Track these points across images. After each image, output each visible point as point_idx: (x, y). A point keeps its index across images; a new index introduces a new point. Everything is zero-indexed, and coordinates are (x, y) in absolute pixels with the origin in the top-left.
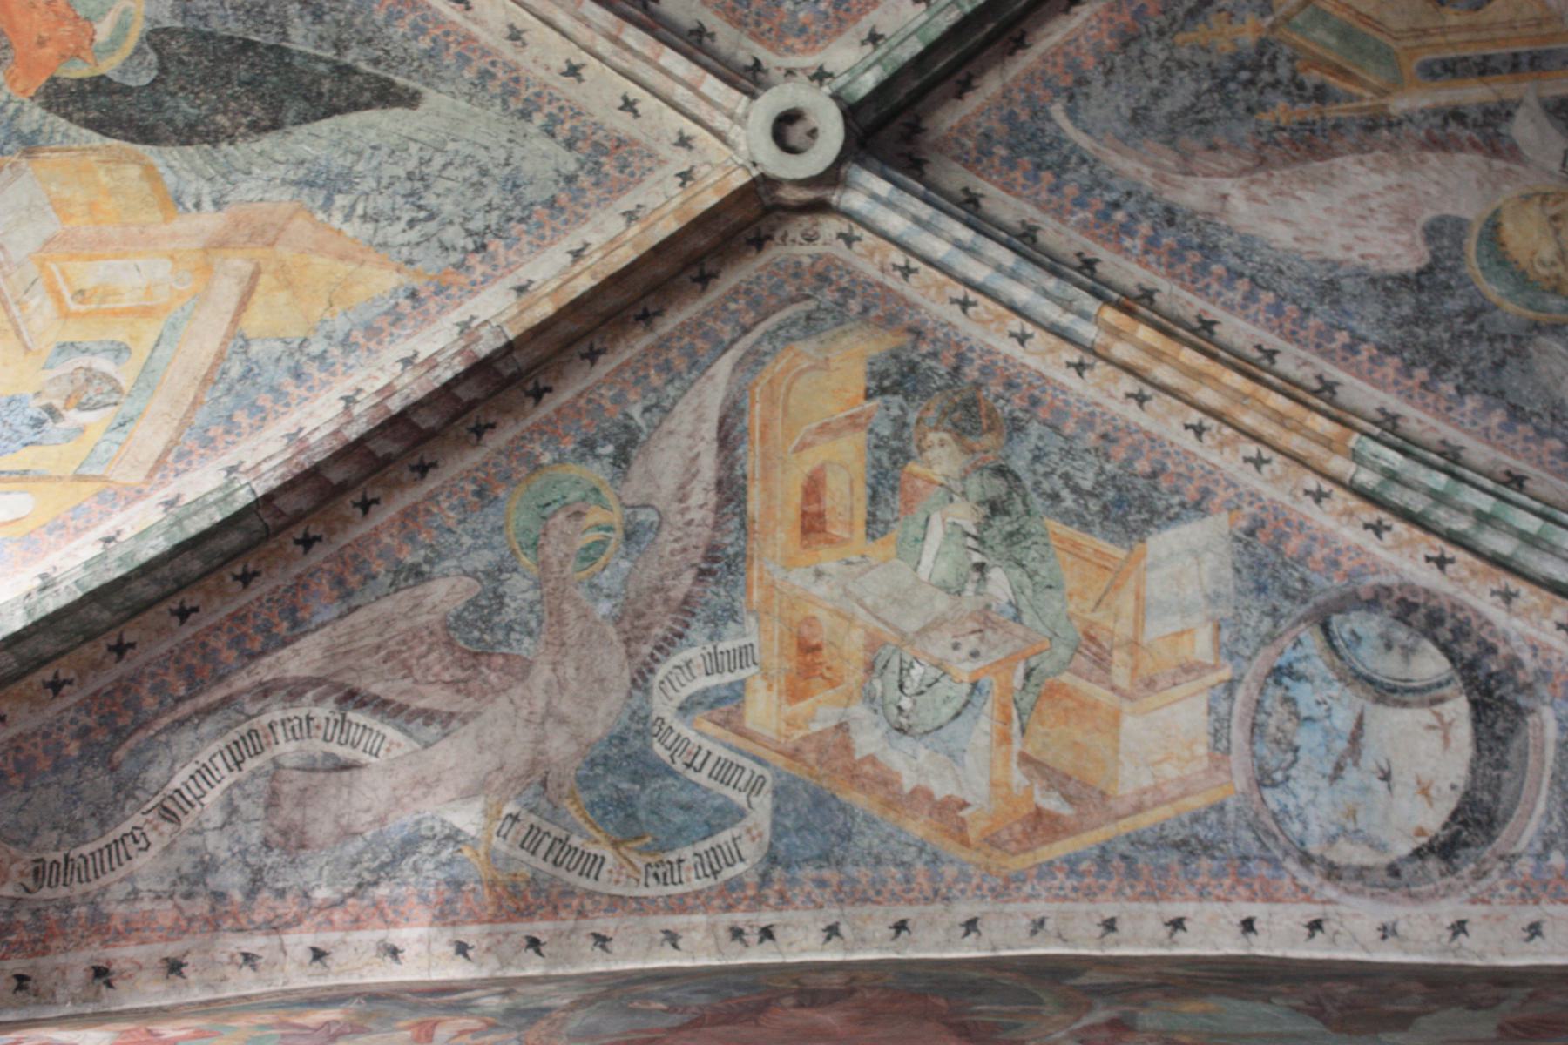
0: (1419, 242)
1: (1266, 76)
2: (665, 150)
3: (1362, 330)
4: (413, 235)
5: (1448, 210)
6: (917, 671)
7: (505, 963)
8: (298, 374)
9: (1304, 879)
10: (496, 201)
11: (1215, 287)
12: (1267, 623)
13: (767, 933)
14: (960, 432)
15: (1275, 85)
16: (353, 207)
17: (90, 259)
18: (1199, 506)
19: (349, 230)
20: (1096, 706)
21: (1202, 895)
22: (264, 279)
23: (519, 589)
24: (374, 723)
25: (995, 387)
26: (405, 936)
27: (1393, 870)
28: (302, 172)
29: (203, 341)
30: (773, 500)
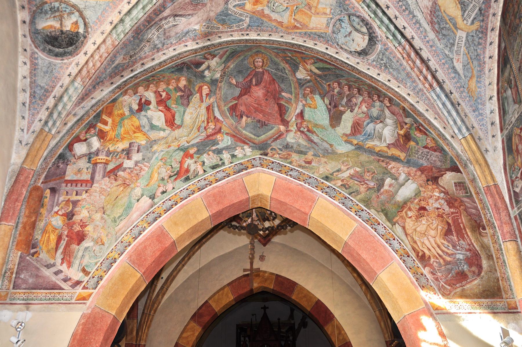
6: (277, 4)
7: (204, 43)
9: (337, 47)
20: (308, 14)
21: (320, 42)
24: (180, 18)
27: (351, 52)
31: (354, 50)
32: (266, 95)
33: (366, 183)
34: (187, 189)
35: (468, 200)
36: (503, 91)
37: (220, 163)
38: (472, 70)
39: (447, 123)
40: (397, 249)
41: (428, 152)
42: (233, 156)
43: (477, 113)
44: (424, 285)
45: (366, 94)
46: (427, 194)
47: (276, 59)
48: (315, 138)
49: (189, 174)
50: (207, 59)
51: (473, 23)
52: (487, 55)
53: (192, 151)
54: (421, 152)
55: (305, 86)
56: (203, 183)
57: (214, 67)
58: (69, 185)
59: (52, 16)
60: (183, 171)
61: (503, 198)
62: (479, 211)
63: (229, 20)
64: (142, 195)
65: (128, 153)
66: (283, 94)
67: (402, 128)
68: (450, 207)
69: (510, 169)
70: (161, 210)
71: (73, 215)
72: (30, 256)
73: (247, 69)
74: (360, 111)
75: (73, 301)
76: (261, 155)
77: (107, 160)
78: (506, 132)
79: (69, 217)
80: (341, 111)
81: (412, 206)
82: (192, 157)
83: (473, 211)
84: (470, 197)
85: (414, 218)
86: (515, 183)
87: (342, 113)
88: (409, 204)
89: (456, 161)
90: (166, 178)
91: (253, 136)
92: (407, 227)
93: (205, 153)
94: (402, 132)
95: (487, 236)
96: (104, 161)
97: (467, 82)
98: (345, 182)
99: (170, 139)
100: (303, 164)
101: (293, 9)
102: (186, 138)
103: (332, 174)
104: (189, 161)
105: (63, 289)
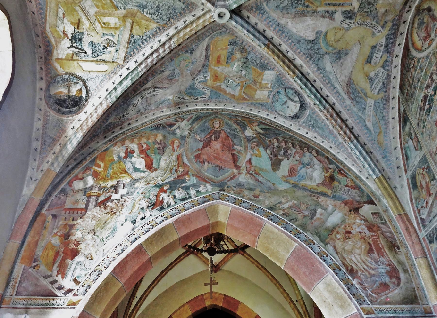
0: (315, 35)
1: (299, 2)
2: (199, 5)
3: (302, 50)
4: (158, 18)
5: (321, 29)
6: (231, 81)
8: (142, 43)
9: (275, 113)
10: (171, 12)
11: (283, 38)
12: (278, 86)
13: (208, 105)
14: (241, 52)
15: (300, 4)
16: (147, 12)
17: (104, 16)
18: (273, 69)
19: (147, 16)
22: (134, 24)
23: (177, 71)
24: (159, 90)
25: (247, 46)
26: (164, 110)
27: (286, 117)
28: (138, 4)
29: (126, 35)
30: (213, 58)
31: (288, 115)
32: (223, 147)
33: (302, 213)
34: (162, 216)
35: (384, 226)
36: (405, 142)
37: (188, 197)
38: (380, 128)
39: (362, 167)
40: (330, 264)
41: (349, 190)
42: (198, 192)
43: (385, 159)
44: (355, 293)
45: (298, 147)
46: (351, 221)
47: (230, 122)
48: (260, 179)
49: (164, 205)
50: (178, 121)
51: (378, 93)
52: (391, 117)
53: (166, 188)
54: (343, 189)
55: (252, 141)
56: (174, 211)
57: (183, 128)
58: (67, 212)
59: (63, 85)
60: (158, 202)
61: (412, 224)
62: (393, 234)
63: (195, 93)
64: (126, 221)
65: (115, 188)
66: (235, 147)
67: (327, 172)
68: (370, 231)
69: (416, 201)
70: (140, 232)
71: (69, 236)
72: (32, 268)
73: (208, 129)
74: (294, 159)
75: (65, 306)
76: (220, 190)
77: (99, 193)
78: (410, 173)
79: (66, 237)
80: (280, 159)
81: (340, 230)
82: (166, 192)
83: (389, 235)
84: (385, 223)
85: (342, 240)
86: (421, 212)
87: (281, 161)
88: (337, 228)
89: (371, 196)
90: (145, 208)
91: (213, 177)
92: (337, 247)
93: (176, 189)
94: (327, 175)
95: (401, 254)
96: (97, 194)
97: (377, 136)
98: (286, 211)
99: (149, 179)
100: (253, 198)
101: (242, 85)
102: (161, 177)
103: (275, 206)
104: (163, 195)
105: (57, 296)
